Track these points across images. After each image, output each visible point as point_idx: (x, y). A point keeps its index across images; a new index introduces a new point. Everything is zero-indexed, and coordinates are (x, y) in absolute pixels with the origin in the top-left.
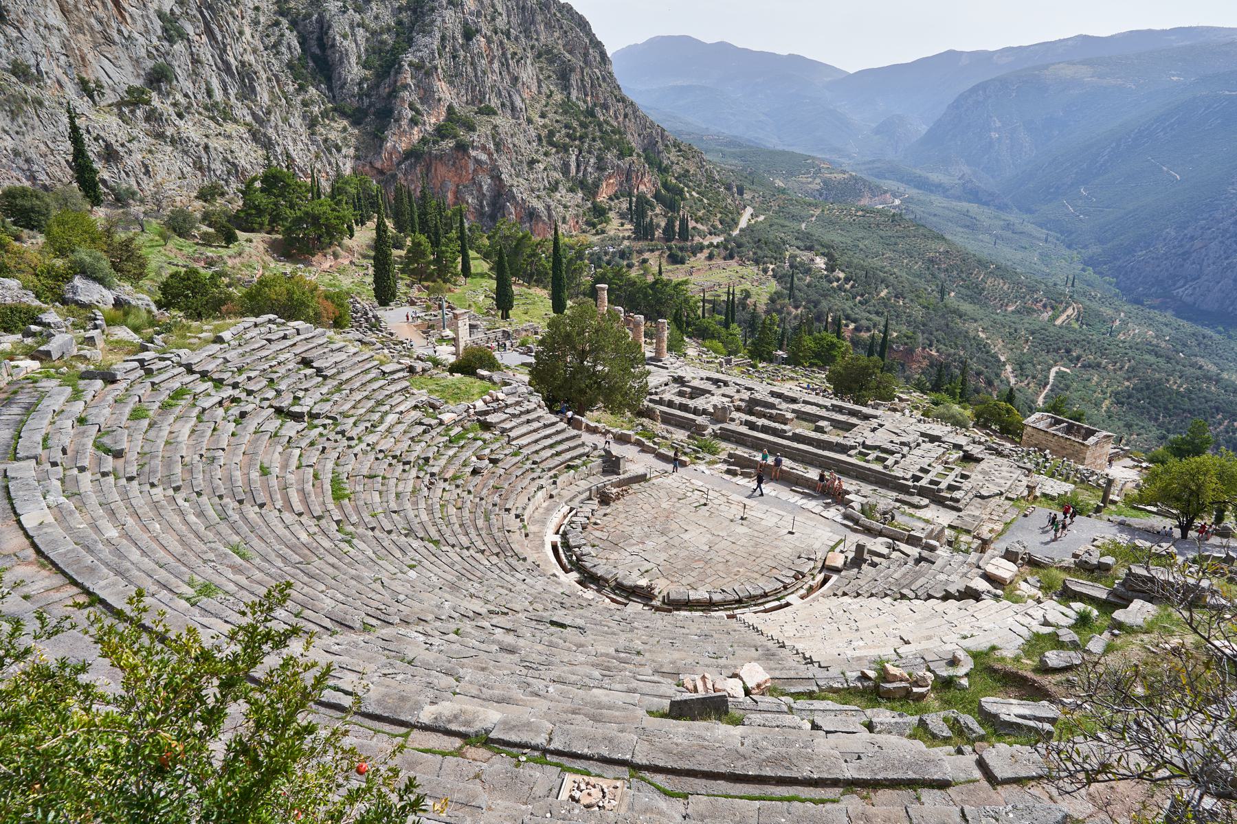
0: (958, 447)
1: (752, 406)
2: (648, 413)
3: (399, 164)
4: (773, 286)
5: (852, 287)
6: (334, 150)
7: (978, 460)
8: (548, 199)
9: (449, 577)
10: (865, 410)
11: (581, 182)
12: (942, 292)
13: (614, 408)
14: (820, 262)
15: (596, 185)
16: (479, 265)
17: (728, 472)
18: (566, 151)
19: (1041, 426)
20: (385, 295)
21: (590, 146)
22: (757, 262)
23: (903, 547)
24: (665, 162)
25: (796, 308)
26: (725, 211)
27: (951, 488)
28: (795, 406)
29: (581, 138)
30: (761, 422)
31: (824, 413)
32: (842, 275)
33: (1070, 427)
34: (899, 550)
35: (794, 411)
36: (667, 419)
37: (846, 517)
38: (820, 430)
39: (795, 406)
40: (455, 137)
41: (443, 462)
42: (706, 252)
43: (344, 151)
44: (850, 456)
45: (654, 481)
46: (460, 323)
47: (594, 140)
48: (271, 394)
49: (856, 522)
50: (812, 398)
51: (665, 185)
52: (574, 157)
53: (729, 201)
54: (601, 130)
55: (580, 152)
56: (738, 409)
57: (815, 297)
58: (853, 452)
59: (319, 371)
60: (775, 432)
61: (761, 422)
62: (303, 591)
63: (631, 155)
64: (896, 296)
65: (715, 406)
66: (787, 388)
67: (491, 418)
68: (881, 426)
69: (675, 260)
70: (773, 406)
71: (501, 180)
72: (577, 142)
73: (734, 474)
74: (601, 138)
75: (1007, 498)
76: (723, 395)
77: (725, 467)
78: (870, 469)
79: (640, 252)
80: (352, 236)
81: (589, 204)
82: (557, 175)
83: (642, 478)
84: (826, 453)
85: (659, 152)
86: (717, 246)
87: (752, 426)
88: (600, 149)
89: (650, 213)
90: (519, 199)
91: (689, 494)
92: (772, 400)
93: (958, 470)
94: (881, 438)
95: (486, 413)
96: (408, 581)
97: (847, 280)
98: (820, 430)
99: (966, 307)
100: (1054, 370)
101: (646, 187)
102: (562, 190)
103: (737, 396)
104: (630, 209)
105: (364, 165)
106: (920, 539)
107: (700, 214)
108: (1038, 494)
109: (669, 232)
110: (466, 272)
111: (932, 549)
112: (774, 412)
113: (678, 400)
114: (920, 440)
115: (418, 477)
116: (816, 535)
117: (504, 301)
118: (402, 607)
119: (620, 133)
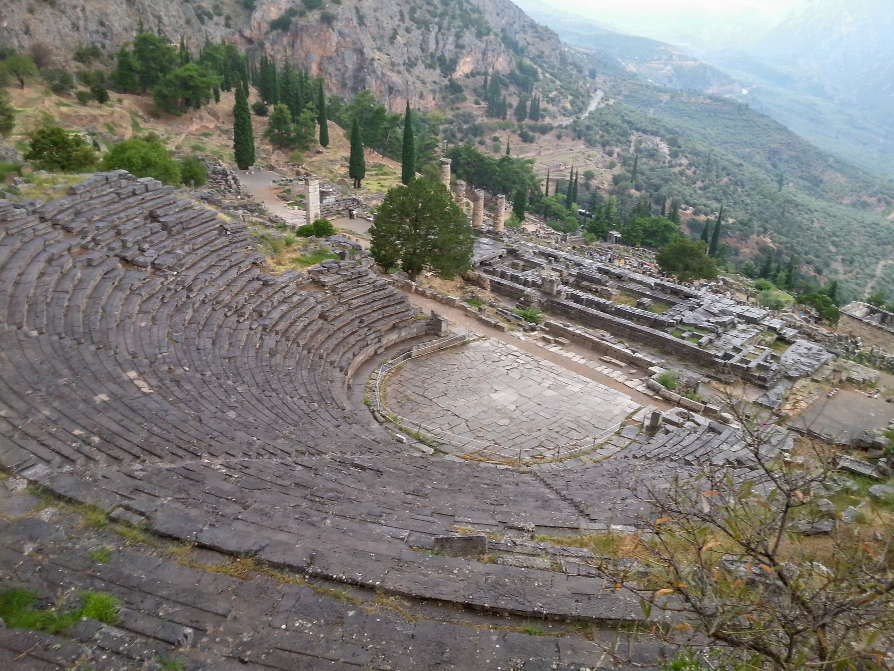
0: (772, 329)
1: (582, 280)
2: (477, 282)
3: (267, 33)
4: (618, 170)
5: (694, 173)
6: (206, 18)
7: (789, 343)
8: (406, 73)
9: (266, 419)
10: (686, 290)
11: (440, 59)
12: (780, 182)
13: (445, 274)
14: (664, 148)
15: (454, 62)
16: (335, 132)
17: (544, 339)
18: (427, 29)
19: (858, 314)
20: (244, 157)
21: (449, 23)
23: (699, 418)
24: (522, 43)
25: (638, 188)
26: (576, 95)
27: (759, 366)
29: (442, 15)
30: (585, 296)
34: (693, 421)
36: (497, 288)
37: (649, 387)
40: (320, 9)
41: (276, 315)
42: (554, 132)
43: (216, 18)
44: (667, 332)
45: (472, 344)
46: (311, 189)
47: (453, 18)
48: (117, 245)
49: (657, 391)
50: (638, 277)
51: (520, 66)
52: (433, 34)
53: (581, 83)
54: (461, 9)
55: (440, 30)
56: (566, 283)
57: (656, 181)
59: (165, 227)
61: (585, 296)
62: (122, 423)
63: (488, 34)
64: (736, 184)
65: (544, 279)
66: (618, 267)
67: (322, 278)
68: (700, 305)
70: (598, 282)
71: (361, 52)
72: (437, 20)
73: (548, 341)
74: (461, 16)
75: (813, 380)
76: (553, 269)
77: (542, 335)
78: (684, 346)
79: (492, 130)
80: (217, 100)
81: (446, 82)
82: (416, 51)
84: (645, 328)
85: (516, 33)
86: (566, 128)
87: (577, 299)
88: (459, 27)
89: (503, 92)
90: (379, 73)
91: (503, 358)
92: (598, 276)
93: (768, 350)
96: (226, 421)
97: (690, 165)
98: (639, 305)
99: (802, 198)
100: (882, 263)
101: (502, 64)
102: (420, 68)
103: (565, 272)
104: (484, 87)
105: (233, 34)
106: (715, 411)
107: (551, 95)
108: (844, 378)
109: (520, 113)
110: (324, 141)
111: (725, 421)
112: (599, 288)
113: (510, 272)
114: (736, 320)
115: (251, 329)
116: (618, 402)
117: (357, 170)
118: (213, 443)
119: (480, 12)
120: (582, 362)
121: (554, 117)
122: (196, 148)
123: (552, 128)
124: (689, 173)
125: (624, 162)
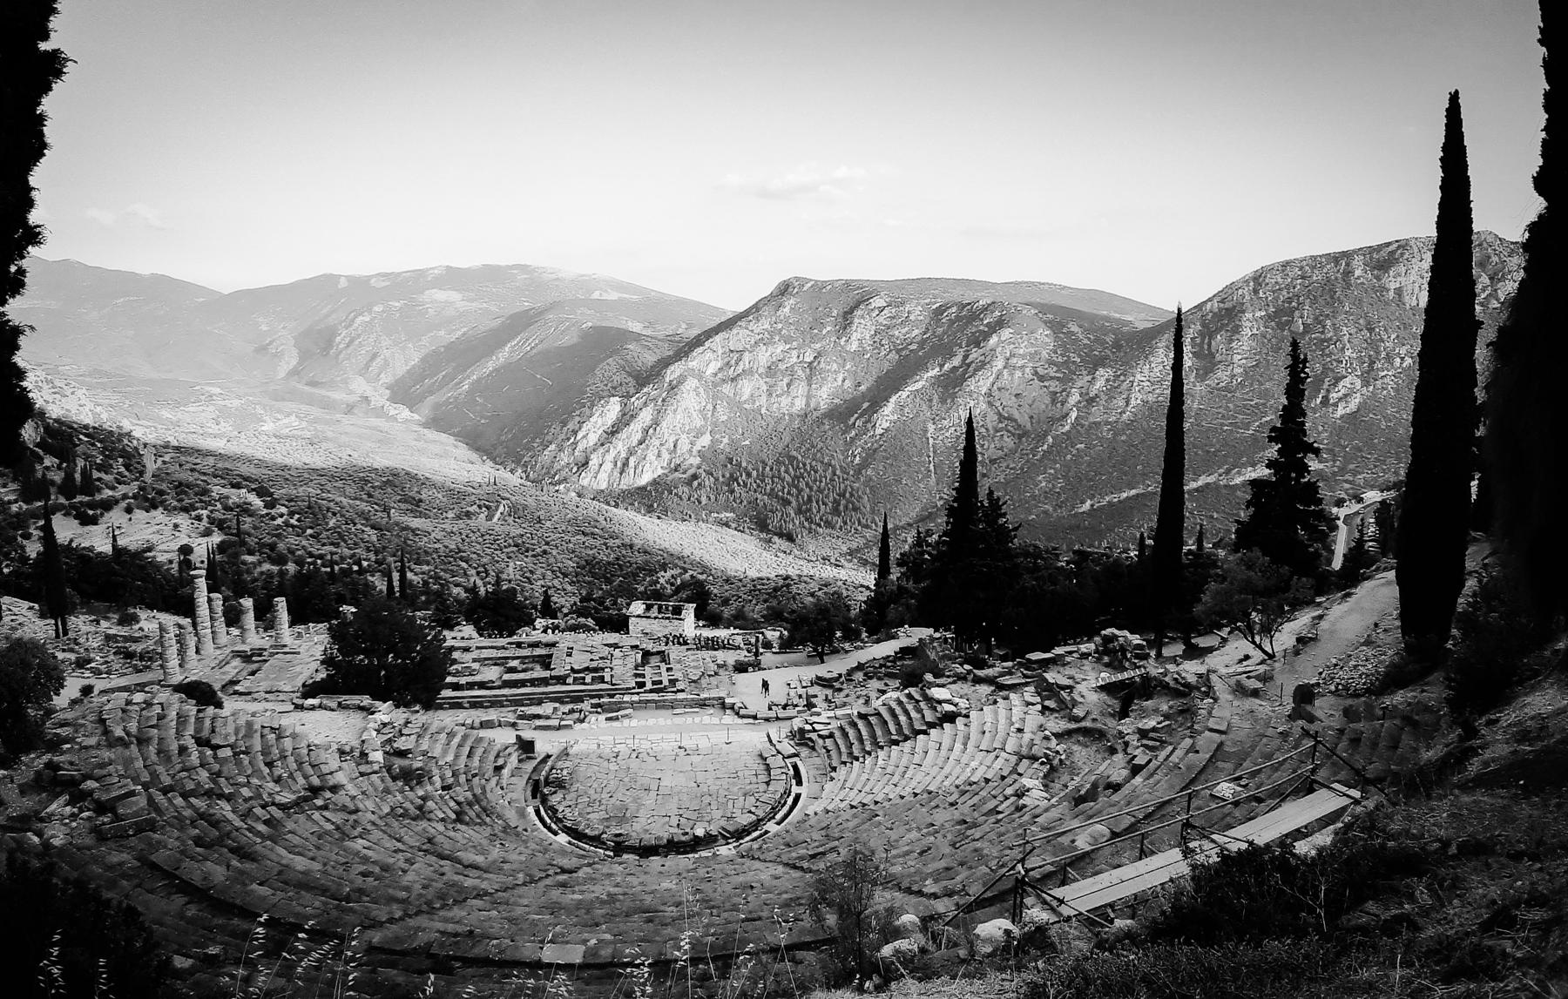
4: (217, 538)
14: (257, 502)
22: (186, 510)
25: (251, 553)
28: (475, 654)
30: (463, 681)
31: (501, 654)
32: (284, 510)
33: (660, 607)
35: (474, 660)
37: (743, 717)
38: (513, 670)
39: (475, 654)
57: (268, 540)
58: (570, 680)
60: (482, 685)
69: (87, 521)
77: (602, 717)
83: (565, 754)
87: (456, 687)
94: (580, 661)
95: (389, 741)
98: (513, 670)
99: (416, 523)
120: (669, 722)
121: (113, 488)
122: (299, 635)
123: (117, 502)
124: (293, 521)
125: (222, 525)
